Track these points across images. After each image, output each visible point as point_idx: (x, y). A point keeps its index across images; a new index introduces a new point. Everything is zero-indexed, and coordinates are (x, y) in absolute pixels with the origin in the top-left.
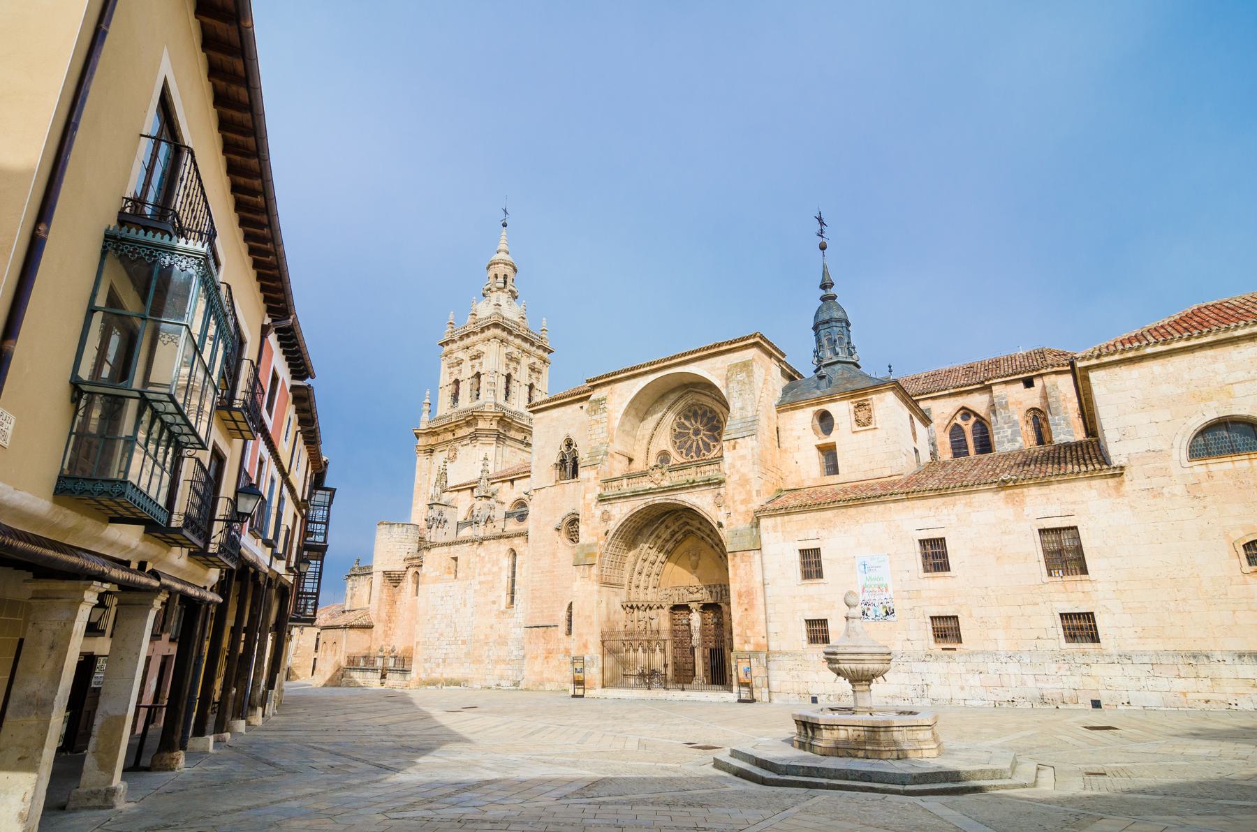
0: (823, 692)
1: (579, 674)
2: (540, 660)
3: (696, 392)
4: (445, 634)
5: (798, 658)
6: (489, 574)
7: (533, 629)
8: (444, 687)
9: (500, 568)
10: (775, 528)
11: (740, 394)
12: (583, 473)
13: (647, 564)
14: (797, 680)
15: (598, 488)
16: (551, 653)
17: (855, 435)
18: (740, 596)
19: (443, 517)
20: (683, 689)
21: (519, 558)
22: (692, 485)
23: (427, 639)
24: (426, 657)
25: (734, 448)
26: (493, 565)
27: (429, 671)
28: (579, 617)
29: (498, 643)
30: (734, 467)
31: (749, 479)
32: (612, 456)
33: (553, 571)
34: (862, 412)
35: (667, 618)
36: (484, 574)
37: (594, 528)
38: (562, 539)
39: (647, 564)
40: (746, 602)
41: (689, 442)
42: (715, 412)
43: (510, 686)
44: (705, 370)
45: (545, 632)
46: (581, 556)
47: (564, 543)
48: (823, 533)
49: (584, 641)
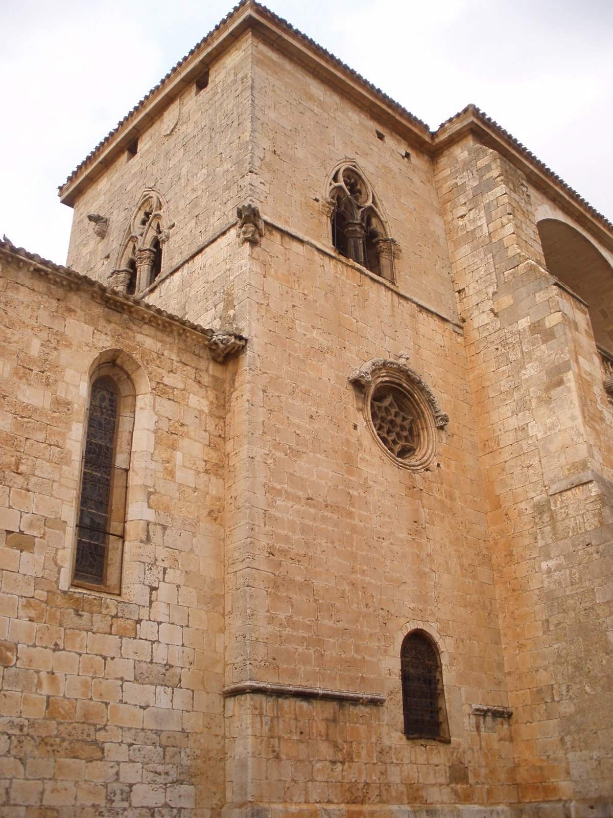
7: (287, 704)
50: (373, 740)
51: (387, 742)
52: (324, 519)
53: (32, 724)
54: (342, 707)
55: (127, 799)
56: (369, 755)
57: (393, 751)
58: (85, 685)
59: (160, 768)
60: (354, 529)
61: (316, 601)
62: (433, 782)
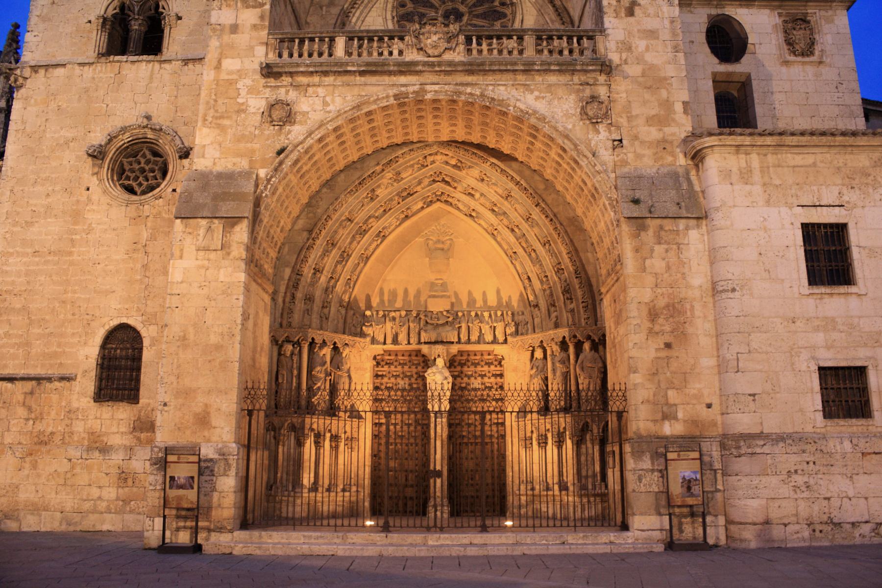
0: (866, 518)
1: (181, 492)
5: (808, 447)
10: (746, 176)
13: (335, 253)
14: (805, 495)
15: (261, 51)
17: (784, 69)
28: (185, 347)
30: (629, 49)
31: (665, 79)
33: (70, 253)
37: (240, 139)
40: (667, 328)
45: (32, 393)
47: (105, 192)
48: (850, 196)
49: (198, 408)
50: (63, 404)
51: (75, 405)
52: (47, 262)
54: (39, 384)
57: (80, 410)
60: (72, 263)
61: (29, 318)
62: (116, 431)
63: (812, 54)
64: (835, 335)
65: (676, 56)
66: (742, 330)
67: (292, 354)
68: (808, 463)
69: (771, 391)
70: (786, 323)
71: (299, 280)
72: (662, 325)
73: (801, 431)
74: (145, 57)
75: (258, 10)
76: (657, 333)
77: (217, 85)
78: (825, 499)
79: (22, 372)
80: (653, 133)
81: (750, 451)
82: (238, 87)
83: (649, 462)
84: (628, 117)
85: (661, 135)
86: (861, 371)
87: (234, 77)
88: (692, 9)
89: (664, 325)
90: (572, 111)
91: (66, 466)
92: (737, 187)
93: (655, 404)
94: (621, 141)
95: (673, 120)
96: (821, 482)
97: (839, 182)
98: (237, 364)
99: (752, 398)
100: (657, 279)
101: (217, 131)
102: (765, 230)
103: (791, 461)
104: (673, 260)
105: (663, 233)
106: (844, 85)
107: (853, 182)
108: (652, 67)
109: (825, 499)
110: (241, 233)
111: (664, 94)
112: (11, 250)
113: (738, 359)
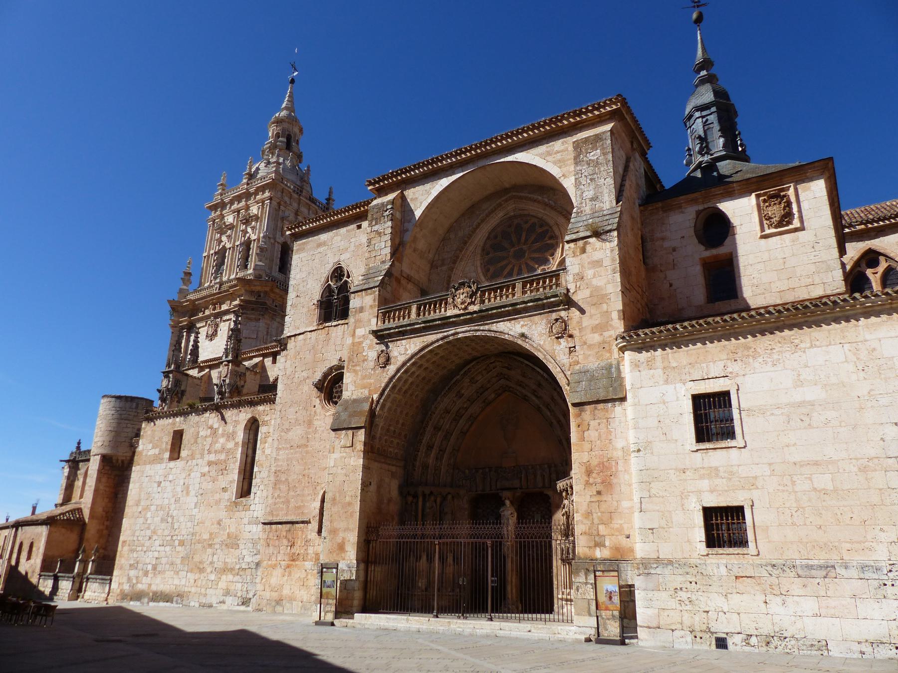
1: (329, 589)
2: (278, 572)
3: (521, 198)
4: (159, 532)
5: (691, 570)
6: (220, 452)
7: (274, 526)
8: (151, 604)
9: (237, 444)
11: (591, 180)
12: (355, 302)
13: (440, 434)
14: (688, 608)
16: (293, 560)
18: (589, 473)
19: (183, 388)
20: (491, 619)
21: (262, 430)
22: (514, 312)
23: (135, 538)
24: (132, 562)
25: (583, 251)
26: (228, 440)
27: (134, 581)
29: (226, 545)
31: (606, 295)
32: (398, 281)
34: (775, 208)
35: (466, 513)
36: (216, 452)
38: (320, 400)
39: (440, 434)
40: (599, 480)
41: (510, 267)
42: (547, 224)
43: (238, 605)
44: (537, 155)
46: (344, 416)
48: (733, 367)
49: (339, 540)
51: (309, 537)
52: (296, 453)
53: (224, 540)
55: (243, 560)
56: (301, 543)
58: (236, 528)
59: (252, 550)
60: (307, 452)
63: (789, 223)
64: (718, 481)
65: (614, 276)
66: (644, 480)
67: (412, 502)
68: (691, 583)
69: (666, 526)
70: (678, 473)
71: (417, 455)
72: (595, 478)
73: (689, 557)
74: (340, 322)
75: (373, 295)
76: (592, 484)
77: (353, 346)
78: (704, 612)
79: (285, 519)
80: (596, 338)
81: (646, 571)
82: (363, 345)
83: (584, 577)
84: (579, 329)
85: (602, 339)
86: (738, 511)
87: (361, 339)
88: (683, 210)
89: (597, 478)
90: (544, 332)
91: (303, 575)
92: (643, 373)
93: (590, 535)
94: (575, 347)
95: (611, 325)
96: (701, 598)
97: (725, 357)
98: (358, 514)
99: (651, 531)
100: (592, 445)
101: (354, 374)
102: (664, 403)
103: (678, 580)
104: (604, 430)
105: (596, 412)
106: (820, 244)
107: (736, 355)
108: (597, 289)
109: (704, 612)
110: (361, 435)
111: (605, 306)
112: (280, 447)
113: (641, 503)
